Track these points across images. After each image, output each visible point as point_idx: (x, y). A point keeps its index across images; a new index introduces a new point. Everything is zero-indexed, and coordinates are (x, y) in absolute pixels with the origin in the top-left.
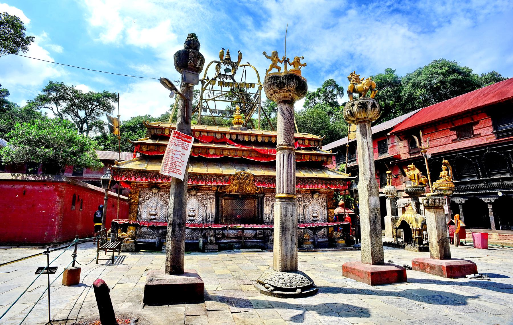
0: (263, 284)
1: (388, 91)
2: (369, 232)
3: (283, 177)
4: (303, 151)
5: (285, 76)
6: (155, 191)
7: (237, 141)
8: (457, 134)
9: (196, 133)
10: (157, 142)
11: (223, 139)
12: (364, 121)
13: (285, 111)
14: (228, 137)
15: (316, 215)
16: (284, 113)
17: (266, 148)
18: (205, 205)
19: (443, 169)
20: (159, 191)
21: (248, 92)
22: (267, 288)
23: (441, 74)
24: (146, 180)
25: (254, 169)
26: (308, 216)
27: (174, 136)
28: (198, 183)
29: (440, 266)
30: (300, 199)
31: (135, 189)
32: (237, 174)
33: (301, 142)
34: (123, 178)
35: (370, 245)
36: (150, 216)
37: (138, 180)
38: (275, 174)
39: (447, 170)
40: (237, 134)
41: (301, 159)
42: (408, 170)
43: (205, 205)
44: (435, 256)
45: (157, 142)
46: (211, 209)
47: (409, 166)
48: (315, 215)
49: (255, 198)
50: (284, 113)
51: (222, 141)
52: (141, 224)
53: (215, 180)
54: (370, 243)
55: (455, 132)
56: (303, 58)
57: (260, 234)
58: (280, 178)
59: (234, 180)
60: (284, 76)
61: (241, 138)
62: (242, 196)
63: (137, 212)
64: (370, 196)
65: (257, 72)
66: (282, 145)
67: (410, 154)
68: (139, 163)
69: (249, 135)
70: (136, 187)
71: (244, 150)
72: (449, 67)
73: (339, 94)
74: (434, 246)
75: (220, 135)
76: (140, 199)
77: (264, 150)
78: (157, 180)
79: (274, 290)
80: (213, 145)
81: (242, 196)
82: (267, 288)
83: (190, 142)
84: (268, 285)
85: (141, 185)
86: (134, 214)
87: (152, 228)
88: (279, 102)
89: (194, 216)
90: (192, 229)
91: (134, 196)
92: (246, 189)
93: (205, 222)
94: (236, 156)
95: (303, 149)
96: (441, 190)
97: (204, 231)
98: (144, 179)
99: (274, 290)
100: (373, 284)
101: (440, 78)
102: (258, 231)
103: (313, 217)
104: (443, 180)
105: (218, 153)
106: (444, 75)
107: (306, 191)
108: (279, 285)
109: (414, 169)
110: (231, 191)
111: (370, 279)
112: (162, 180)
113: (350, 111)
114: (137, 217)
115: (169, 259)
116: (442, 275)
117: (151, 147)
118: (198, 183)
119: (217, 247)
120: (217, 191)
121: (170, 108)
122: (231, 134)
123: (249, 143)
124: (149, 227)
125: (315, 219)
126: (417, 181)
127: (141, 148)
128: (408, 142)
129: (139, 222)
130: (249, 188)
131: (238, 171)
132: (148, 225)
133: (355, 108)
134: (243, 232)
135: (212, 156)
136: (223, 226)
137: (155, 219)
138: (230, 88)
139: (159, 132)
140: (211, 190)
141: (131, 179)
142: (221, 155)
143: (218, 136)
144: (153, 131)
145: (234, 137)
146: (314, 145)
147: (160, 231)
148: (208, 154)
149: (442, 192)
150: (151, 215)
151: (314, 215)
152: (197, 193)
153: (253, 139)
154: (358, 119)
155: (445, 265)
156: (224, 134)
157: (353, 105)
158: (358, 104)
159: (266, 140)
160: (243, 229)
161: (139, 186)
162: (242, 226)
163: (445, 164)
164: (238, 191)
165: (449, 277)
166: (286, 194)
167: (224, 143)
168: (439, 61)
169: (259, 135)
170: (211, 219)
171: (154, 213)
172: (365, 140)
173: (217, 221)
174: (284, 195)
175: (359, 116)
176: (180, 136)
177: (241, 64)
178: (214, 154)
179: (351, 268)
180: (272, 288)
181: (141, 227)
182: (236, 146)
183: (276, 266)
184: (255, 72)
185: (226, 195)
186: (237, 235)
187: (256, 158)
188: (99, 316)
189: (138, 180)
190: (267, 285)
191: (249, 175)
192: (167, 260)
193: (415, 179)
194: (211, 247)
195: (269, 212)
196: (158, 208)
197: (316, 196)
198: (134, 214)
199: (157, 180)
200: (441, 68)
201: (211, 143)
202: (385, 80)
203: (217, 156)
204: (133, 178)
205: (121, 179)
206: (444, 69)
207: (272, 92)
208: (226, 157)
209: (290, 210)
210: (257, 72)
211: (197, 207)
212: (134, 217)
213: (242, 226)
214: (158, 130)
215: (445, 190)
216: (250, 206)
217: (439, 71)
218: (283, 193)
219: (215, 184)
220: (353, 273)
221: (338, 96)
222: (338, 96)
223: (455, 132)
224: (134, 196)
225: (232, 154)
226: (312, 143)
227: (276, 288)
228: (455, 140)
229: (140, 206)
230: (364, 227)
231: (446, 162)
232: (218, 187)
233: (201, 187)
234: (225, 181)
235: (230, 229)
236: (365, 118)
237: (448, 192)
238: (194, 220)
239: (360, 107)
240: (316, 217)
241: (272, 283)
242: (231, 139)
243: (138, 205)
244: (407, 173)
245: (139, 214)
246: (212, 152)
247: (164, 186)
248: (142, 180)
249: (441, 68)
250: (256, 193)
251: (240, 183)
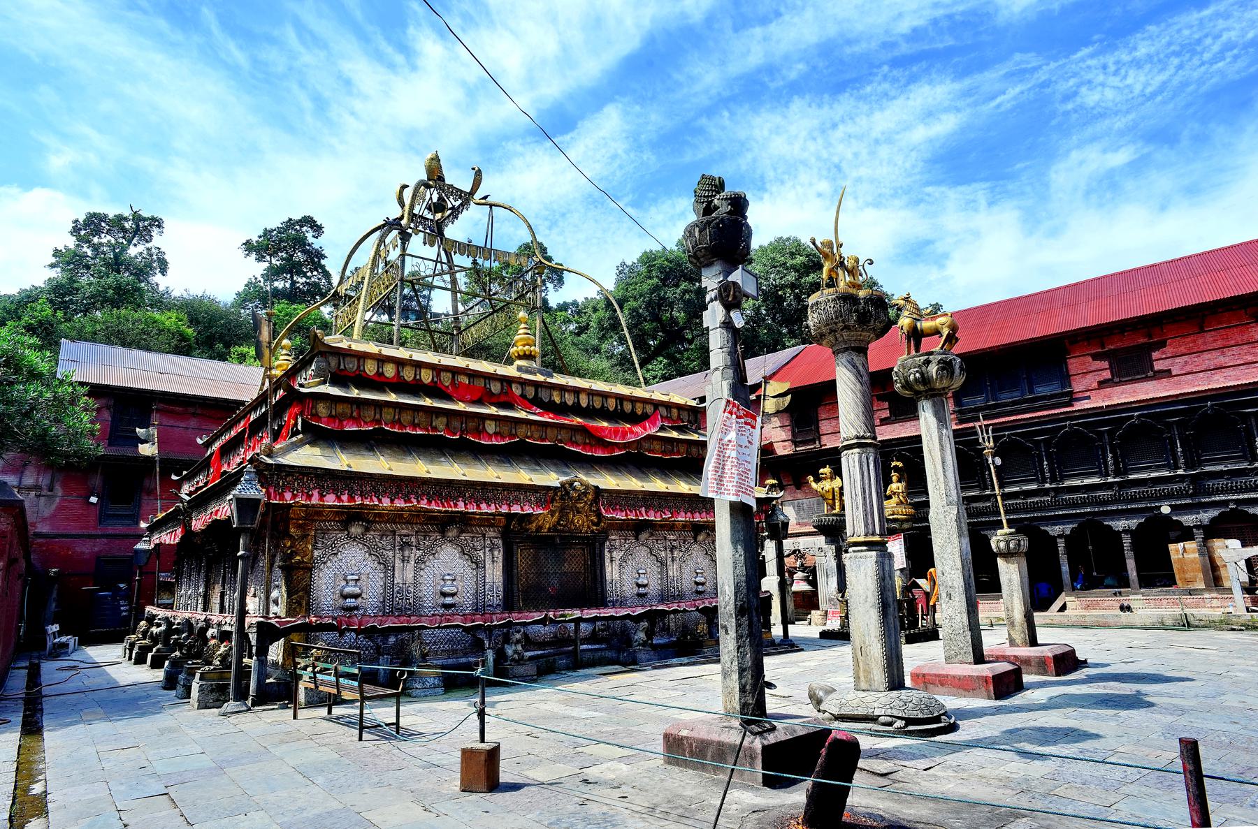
0: (874, 719)
1: (685, 292)
2: (964, 604)
3: (871, 501)
4: (675, 434)
5: (870, 299)
6: (356, 530)
7: (536, 402)
8: (890, 409)
9: (443, 374)
10: (355, 393)
11: (505, 393)
12: (941, 395)
13: (861, 368)
14: (516, 390)
15: (702, 580)
16: (858, 371)
17: (605, 424)
18: (478, 565)
19: (894, 479)
20: (367, 530)
21: (316, 246)
22: (890, 724)
23: (794, 268)
24: (351, 499)
25: (587, 474)
26: (687, 584)
27: (731, 413)
28: (479, 507)
29: (1040, 658)
30: (675, 544)
31: (299, 527)
32: (563, 485)
33: (663, 411)
34: (288, 496)
35: (967, 629)
36: (341, 602)
37: (330, 500)
38: (704, 488)
39: (899, 481)
40: (537, 385)
41: (672, 453)
42: (818, 480)
43: (478, 565)
44: (1019, 641)
45: (355, 393)
46: (494, 573)
47: (821, 471)
48: (700, 579)
49: (587, 545)
50: (858, 371)
51: (503, 399)
52: (340, 623)
53: (517, 501)
54: (966, 623)
55: (886, 405)
56: (871, 263)
57: (603, 630)
58: (864, 504)
59: (553, 500)
60: (867, 300)
61: (544, 394)
62: (562, 538)
63: (307, 590)
64: (960, 536)
65: (530, 227)
66: (863, 437)
67: (796, 444)
68: (317, 451)
69: (563, 389)
70: (305, 519)
71: (562, 426)
72: (807, 256)
73: (552, 282)
74: (1017, 623)
75: (498, 385)
76: (316, 553)
77: (602, 429)
78: (380, 501)
79: (906, 725)
80: (493, 410)
81: (562, 538)
82: (890, 724)
83: (754, 427)
84: (889, 719)
85: (319, 514)
86: (301, 598)
87: (370, 632)
88: (846, 350)
89: (453, 595)
90: (466, 629)
91: (300, 546)
92: (573, 521)
93: (480, 608)
94: (543, 440)
95: (673, 428)
96: (895, 520)
97: (496, 632)
98: (345, 498)
99: (906, 725)
100: (999, 696)
101: (791, 277)
102: (599, 623)
103: (697, 584)
104: (895, 499)
105: (505, 429)
106: (796, 271)
107: (684, 526)
108: (913, 715)
109: (832, 479)
110: (539, 528)
111: (991, 688)
112: (392, 501)
113: (922, 374)
114: (308, 603)
115: (748, 687)
116: (1045, 673)
117: (340, 408)
118: (479, 507)
119: (530, 669)
120: (506, 527)
121: (53, 260)
122: (524, 383)
123: (562, 409)
124: (358, 632)
125: (700, 588)
126: (837, 504)
127: (314, 407)
128: (792, 416)
129: (334, 618)
130: (578, 520)
131: (564, 479)
132: (360, 624)
133: (933, 369)
134: (577, 629)
135: (490, 437)
136: (538, 616)
137: (356, 608)
138: (471, 259)
139: (351, 365)
140: (492, 525)
141: (309, 497)
142: (512, 436)
143: (495, 388)
144: (333, 362)
145: (530, 392)
146: (689, 421)
147: (392, 640)
148: (480, 431)
149: (896, 525)
150: (345, 597)
151: (698, 579)
152: (462, 532)
153: (570, 399)
154: (933, 389)
155: (1050, 655)
156: (507, 381)
157: (928, 362)
158: (939, 362)
159: (597, 404)
160: (578, 621)
161: (314, 514)
162: (577, 613)
163: (896, 469)
164: (553, 529)
165: (1058, 675)
166: (881, 535)
167: (509, 406)
168: (788, 239)
169: (584, 390)
170: (496, 601)
171: (357, 590)
172: (944, 431)
173: (509, 604)
174: (877, 538)
175: (938, 385)
176: (742, 413)
177: (477, 196)
178: (496, 434)
179: (936, 676)
180: (899, 724)
181: (342, 633)
182: (538, 414)
183: (870, 681)
184: (525, 226)
185: (529, 537)
186: (555, 636)
187: (585, 446)
188: (803, 811)
189: (330, 500)
190: (882, 719)
191: (587, 487)
192: (742, 690)
193: (834, 499)
194: (521, 670)
195: (616, 576)
196: (363, 577)
197: (701, 538)
198: (301, 598)
199: (380, 501)
200: (792, 255)
201: (479, 402)
202: (680, 265)
203: (503, 438)
204: (316, 493)
205: (282, 498)
206: (799, 260)
207: (841, 325)
208: (522, 442)
209: (887, 568)
210: (530, 227)
211: (459, 571)
212: (300, 604)
213: (577, 613)
214: (348, 359)
215: (902, 521)
216: (573, 563)
217: (790, 262)
218: (874, 534)
219: (516, 509)
220: (942, 685)
221: (550, 286)
222: (550, 286)
223: (886, 405)
224: (300, 546)
225: (536, 435)
226: (685, 415)
227: (909, 721)
228: (886, 419)
229: (316, 573)
230: (950, 596)
231: (900, 464)
232: (510, 516)
233: (471, 519)
234: (539, 503)
235: (552, 621)
236: (943, 389)
237: (906, 526)
238: (453, 605)
239: (942, 369)
240: (703, 584)
241: (895, 713)
242: (523, 396)
243: (310, 570)
244: (814, 485)
245: (314, 595)
246: (491, 427)
247: (380, 515)
248: (339, 499)
249: (792, 255)
250: (592, 532)
251: (562, 510)
